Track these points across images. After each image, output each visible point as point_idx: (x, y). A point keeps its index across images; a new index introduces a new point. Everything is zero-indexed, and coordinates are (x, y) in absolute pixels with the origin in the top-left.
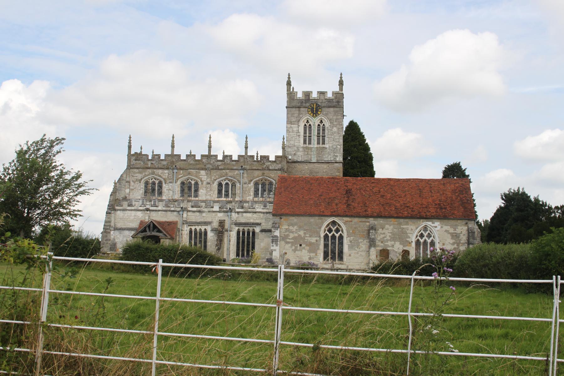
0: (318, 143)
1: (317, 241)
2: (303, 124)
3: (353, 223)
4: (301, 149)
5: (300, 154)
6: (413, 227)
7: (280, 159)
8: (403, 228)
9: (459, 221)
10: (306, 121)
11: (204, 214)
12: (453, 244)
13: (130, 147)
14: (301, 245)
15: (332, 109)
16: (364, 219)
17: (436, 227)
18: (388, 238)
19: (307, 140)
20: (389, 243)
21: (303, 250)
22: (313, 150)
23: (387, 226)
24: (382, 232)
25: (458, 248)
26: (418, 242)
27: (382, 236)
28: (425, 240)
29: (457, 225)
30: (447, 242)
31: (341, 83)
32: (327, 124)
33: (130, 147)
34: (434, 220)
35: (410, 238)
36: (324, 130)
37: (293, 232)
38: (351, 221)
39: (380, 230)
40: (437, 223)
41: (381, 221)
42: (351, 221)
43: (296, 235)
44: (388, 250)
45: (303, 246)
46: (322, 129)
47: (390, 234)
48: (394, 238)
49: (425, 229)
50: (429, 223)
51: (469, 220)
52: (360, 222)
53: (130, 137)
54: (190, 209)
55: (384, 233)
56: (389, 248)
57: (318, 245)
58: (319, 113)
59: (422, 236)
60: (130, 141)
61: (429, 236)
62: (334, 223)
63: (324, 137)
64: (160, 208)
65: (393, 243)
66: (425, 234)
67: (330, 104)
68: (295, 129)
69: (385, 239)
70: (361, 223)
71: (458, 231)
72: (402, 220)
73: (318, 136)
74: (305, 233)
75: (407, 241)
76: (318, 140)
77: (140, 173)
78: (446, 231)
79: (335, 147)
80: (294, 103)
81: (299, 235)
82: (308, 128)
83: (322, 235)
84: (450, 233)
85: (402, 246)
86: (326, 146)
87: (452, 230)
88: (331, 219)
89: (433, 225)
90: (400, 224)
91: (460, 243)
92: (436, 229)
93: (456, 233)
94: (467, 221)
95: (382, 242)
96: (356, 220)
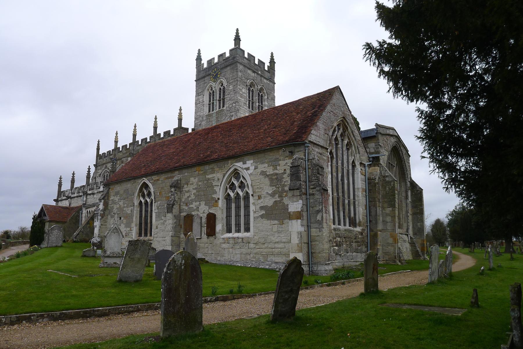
0: (220, 108)
1: (131, 211)
2: (208, 93)
3: (160, 182)
4: (205, 119)
5: (204, 123)
6: (219, 175)
7: (176, 131)
8: (209, 179)
9: (281, 152)
10: (210, 89)
11: (95, 196)
12: (273, 195)
13: (98, 149)
14: (120, 218)
15: (229, 68)
16: (169, 175)
17: (247, 169)
18: (193, 197)
19: (211, 106)
20: (194, 205)
21: (122, 225)
22: (214, 115)
23: (192, 179)
24: (187, 189)
25: (280, 202)
26: (228, 198)
27: (187, 195)
28: (238, 194)
29: (277, 160)
30: (264, 193)
31: (237, 39)
32: (225, 84)
33: (98, 149)
34: (246, 158)
35: (216, 193)
36: (224, 92)
37: (115, 203)
38: (158, 180)
39: (185, 186)
40: (249, 163)
41: (186, 173)
42: (158, 180)
43: (118, 206)
44: (193, 216)
45: (122, 219)
46: (223, 91)
47: (195, 191)
48: (198, 198)
49: (236, 174)
50: (239, 165)
51: (295, 146)
52: (167, 178)
53: (99, 142)
54: (89, 192)
55: (189, 191)
56: (193, 213)
57: (131, 216)
58: (219, 76)
59: (232, 187)
60: (98, 144)
61: (242, 186)
62: (145, 185)
63: (224, 99)
64: (76, 195)
65: (198, 203)
66: (237, 184)
67: (227, 63)
68: (201, 100)
69: (190, 199)
70: (167, 181)
71: (280, 170)
72: (207, 167)
73: (220, 101)
74: (124, 204)
75: (213, 199)
76: (220, 104)
77: (101, 169)
78: (263, 173)
79: (231, 106)
80: (202, 75)
81: (120, 206)
82: (212, 95)
83: (136, 203)
84: (268, 176)
85: (207, 207)
86: (225, 108)
87: (270, 171)
88: (141, 182)
89: (245, 166)
90: (205, 173)
91: (283, 191)
92: (250, 172)
93: (277, 174)
94: (292, 149)
95: (187, 205)
96: (163, 177)
